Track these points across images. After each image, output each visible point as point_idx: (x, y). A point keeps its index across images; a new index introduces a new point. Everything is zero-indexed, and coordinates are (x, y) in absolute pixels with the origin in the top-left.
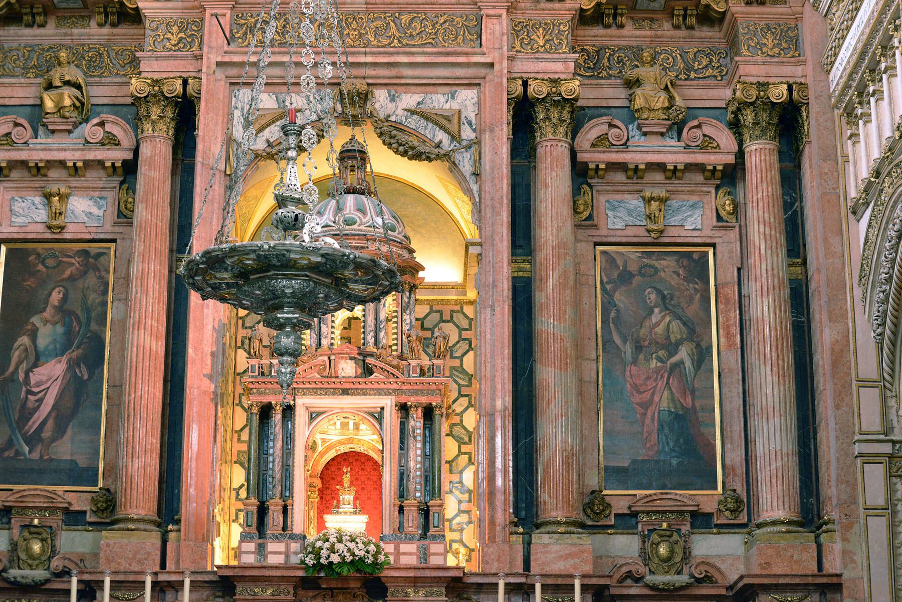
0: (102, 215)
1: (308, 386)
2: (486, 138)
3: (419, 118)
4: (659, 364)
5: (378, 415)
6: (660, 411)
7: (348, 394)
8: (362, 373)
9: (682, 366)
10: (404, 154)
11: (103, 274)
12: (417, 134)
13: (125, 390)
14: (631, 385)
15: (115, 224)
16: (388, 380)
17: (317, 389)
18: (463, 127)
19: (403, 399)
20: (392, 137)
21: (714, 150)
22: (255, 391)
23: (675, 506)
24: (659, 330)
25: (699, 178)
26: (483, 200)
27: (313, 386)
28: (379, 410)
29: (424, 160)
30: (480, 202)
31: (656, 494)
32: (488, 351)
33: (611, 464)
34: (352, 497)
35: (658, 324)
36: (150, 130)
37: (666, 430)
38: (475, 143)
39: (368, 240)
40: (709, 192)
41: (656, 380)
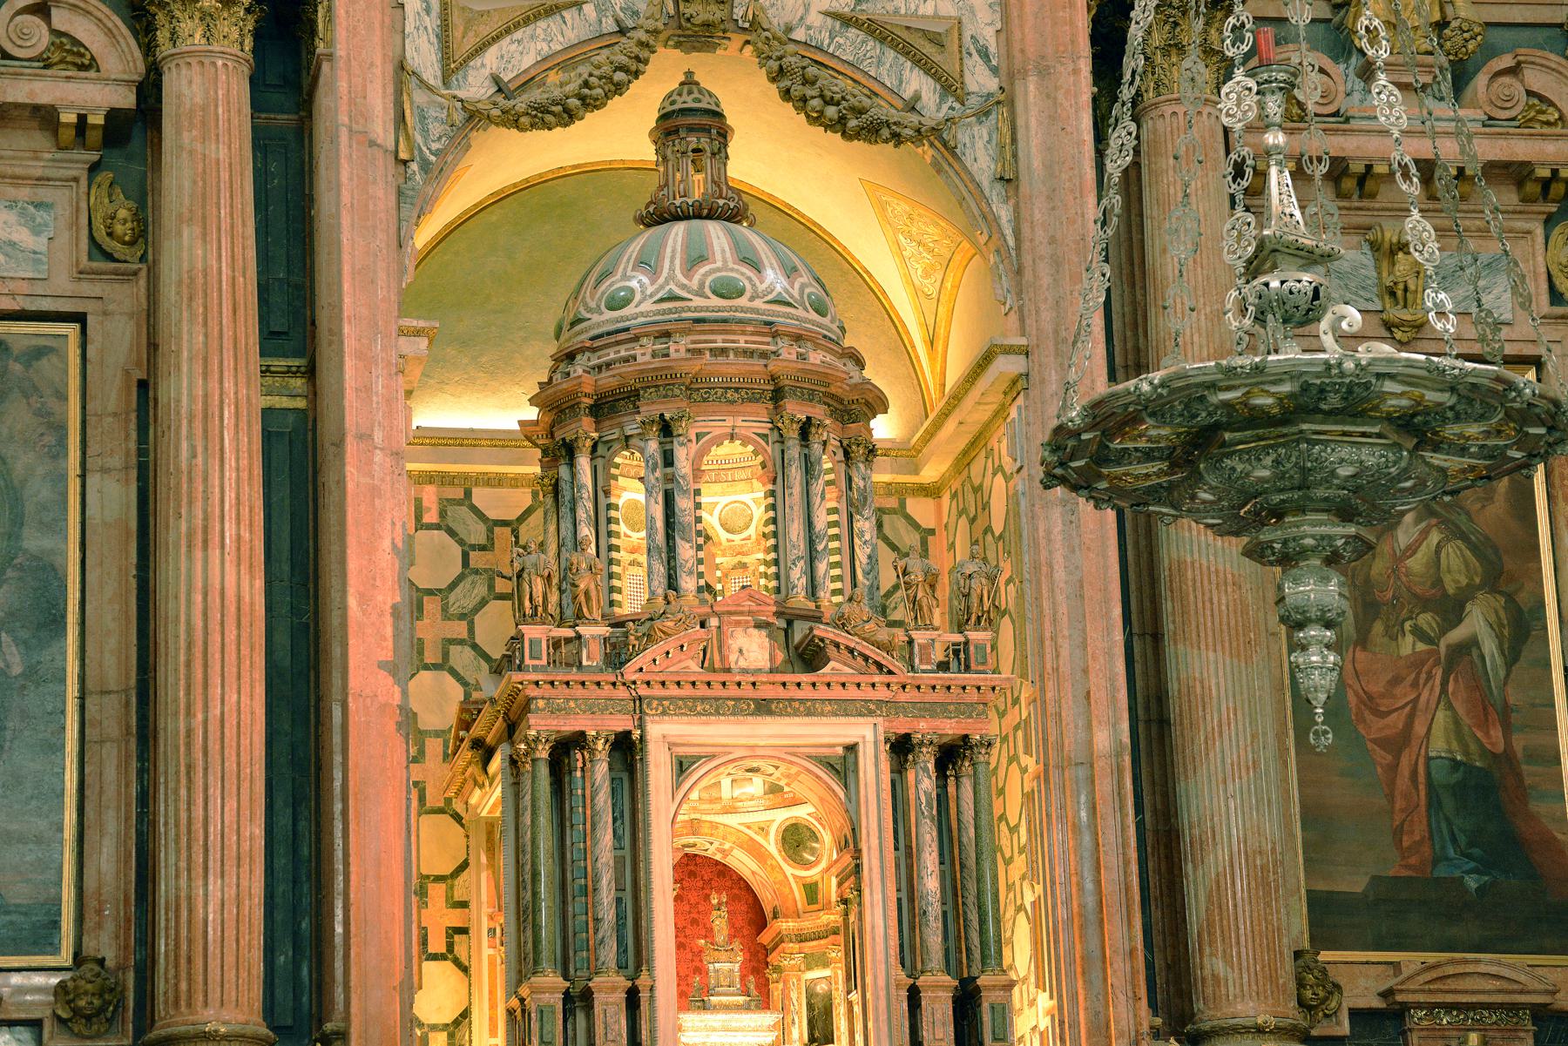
0: (44, 249)
1: (673, 691)
2: (1030, 91)
3: (862, 36)
4: (1421, 646)
5: (843, 765)
6: (1429, 759)
7: (770, 713)
8: (785, 662)
9: (1475, 652)
10: (838, 125)
11: (52, 403)
12: (858, 76)
13: (176, 700)
14: (1356, 694)
15: (82, 274)
16: (862, 679)
17: (695, 699)
18: (968, 62)
19: (902, 726)
20: (807, 82)
21: (1546, 130)
22: (541, 703)
23: (1500, 991)
24: (1417, 563)
25: (1511, 197)
26: (1026, 245)
27: (687, 691)
28: (840, 750)
29: (886, 141)
30: (1018, 248)
31: (1452, 962)
32: (1063, 609)
33: (1321, 886)
34: (737, 967)
35: (1412, 550)
36: (198, 36)
37: (1449, 804)
38: (998, 103)
39: (775, 335)
40: (1529, 232)
41: (1415, 684)
